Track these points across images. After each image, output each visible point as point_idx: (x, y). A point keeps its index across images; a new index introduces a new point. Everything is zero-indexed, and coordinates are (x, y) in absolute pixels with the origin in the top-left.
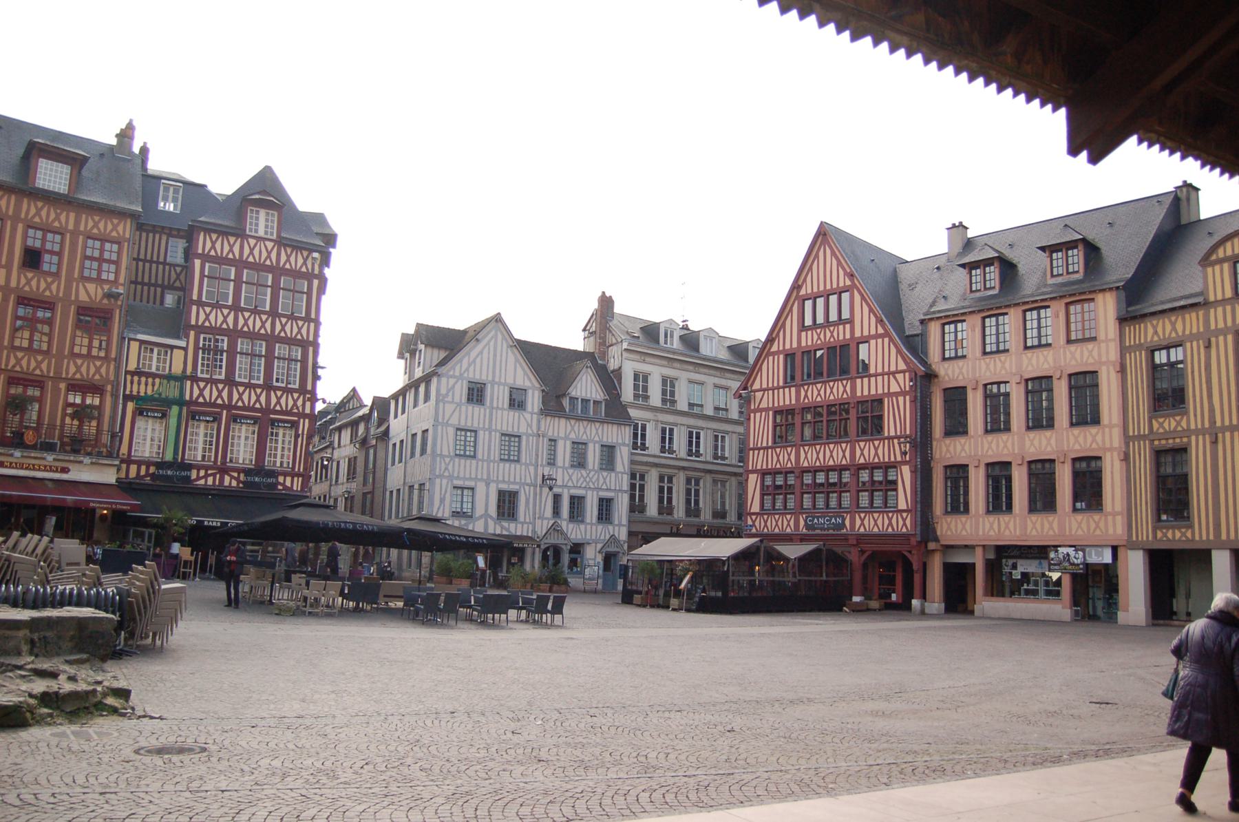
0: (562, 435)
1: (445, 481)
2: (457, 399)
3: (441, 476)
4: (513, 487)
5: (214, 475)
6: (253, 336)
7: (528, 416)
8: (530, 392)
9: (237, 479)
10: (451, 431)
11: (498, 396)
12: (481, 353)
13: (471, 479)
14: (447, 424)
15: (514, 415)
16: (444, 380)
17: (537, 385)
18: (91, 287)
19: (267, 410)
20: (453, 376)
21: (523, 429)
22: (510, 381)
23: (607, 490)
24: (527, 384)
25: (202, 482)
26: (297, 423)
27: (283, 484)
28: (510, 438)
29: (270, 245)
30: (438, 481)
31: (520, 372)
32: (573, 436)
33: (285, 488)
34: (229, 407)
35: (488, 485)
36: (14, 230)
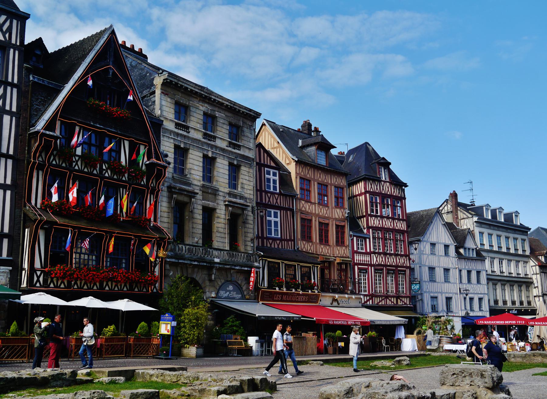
0: (463, 267)
1: (427, 294)
2: (427, 253)
3: (426, 292)
4: (450, 295)
5: (384, 299)
6: (388, 230)
7: (451, 259)
8: (451, 247)
9: (391, 300)
10: (427, 269)
11: (440, 249)
12: (433, 228)
13: (436, 292)
14: (425, 265)
15: (446, 258)
16: (422, 243)
17: (453, 243)
18: (338, 210)
19: (397, 266)
20: (425, 241)
21: (450, 266)
22: (444, 242)
23: (481, 294)
24: (450, 243)
25: (381, 303)
26: (405, 271)
27: (404, 302)
28: (447, 270)
29: (388, 184)
30: (425, 294)
31: (447, 237)
32: (467, 267)
33: (405, 304)
34: (386, 266)
35: (442, 295)
36: (314, 185)
